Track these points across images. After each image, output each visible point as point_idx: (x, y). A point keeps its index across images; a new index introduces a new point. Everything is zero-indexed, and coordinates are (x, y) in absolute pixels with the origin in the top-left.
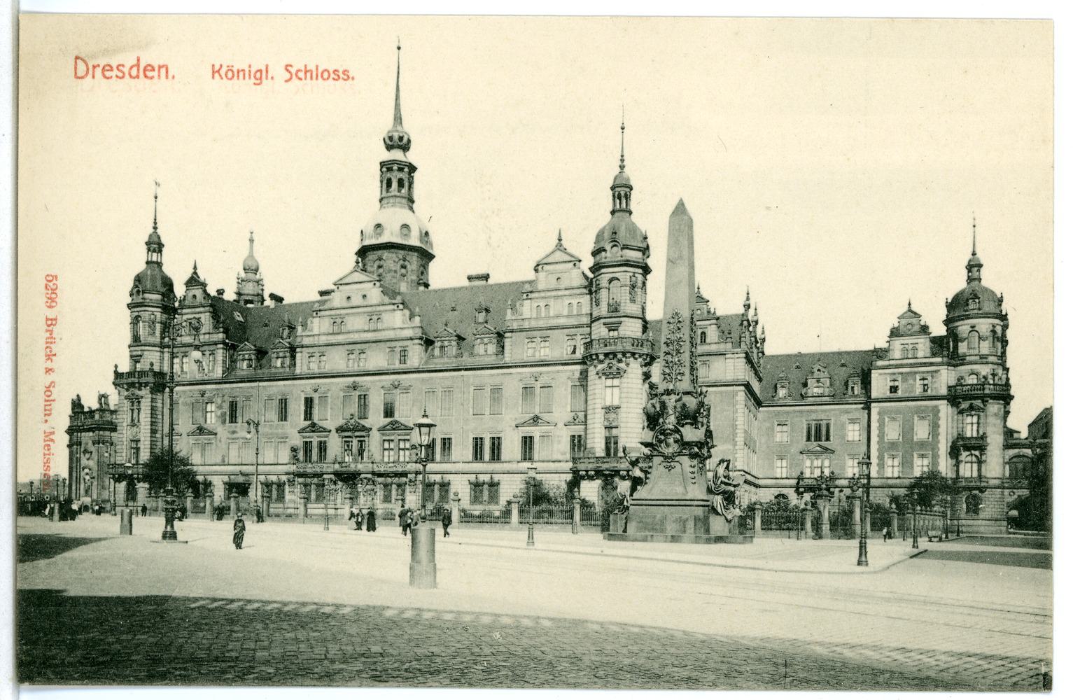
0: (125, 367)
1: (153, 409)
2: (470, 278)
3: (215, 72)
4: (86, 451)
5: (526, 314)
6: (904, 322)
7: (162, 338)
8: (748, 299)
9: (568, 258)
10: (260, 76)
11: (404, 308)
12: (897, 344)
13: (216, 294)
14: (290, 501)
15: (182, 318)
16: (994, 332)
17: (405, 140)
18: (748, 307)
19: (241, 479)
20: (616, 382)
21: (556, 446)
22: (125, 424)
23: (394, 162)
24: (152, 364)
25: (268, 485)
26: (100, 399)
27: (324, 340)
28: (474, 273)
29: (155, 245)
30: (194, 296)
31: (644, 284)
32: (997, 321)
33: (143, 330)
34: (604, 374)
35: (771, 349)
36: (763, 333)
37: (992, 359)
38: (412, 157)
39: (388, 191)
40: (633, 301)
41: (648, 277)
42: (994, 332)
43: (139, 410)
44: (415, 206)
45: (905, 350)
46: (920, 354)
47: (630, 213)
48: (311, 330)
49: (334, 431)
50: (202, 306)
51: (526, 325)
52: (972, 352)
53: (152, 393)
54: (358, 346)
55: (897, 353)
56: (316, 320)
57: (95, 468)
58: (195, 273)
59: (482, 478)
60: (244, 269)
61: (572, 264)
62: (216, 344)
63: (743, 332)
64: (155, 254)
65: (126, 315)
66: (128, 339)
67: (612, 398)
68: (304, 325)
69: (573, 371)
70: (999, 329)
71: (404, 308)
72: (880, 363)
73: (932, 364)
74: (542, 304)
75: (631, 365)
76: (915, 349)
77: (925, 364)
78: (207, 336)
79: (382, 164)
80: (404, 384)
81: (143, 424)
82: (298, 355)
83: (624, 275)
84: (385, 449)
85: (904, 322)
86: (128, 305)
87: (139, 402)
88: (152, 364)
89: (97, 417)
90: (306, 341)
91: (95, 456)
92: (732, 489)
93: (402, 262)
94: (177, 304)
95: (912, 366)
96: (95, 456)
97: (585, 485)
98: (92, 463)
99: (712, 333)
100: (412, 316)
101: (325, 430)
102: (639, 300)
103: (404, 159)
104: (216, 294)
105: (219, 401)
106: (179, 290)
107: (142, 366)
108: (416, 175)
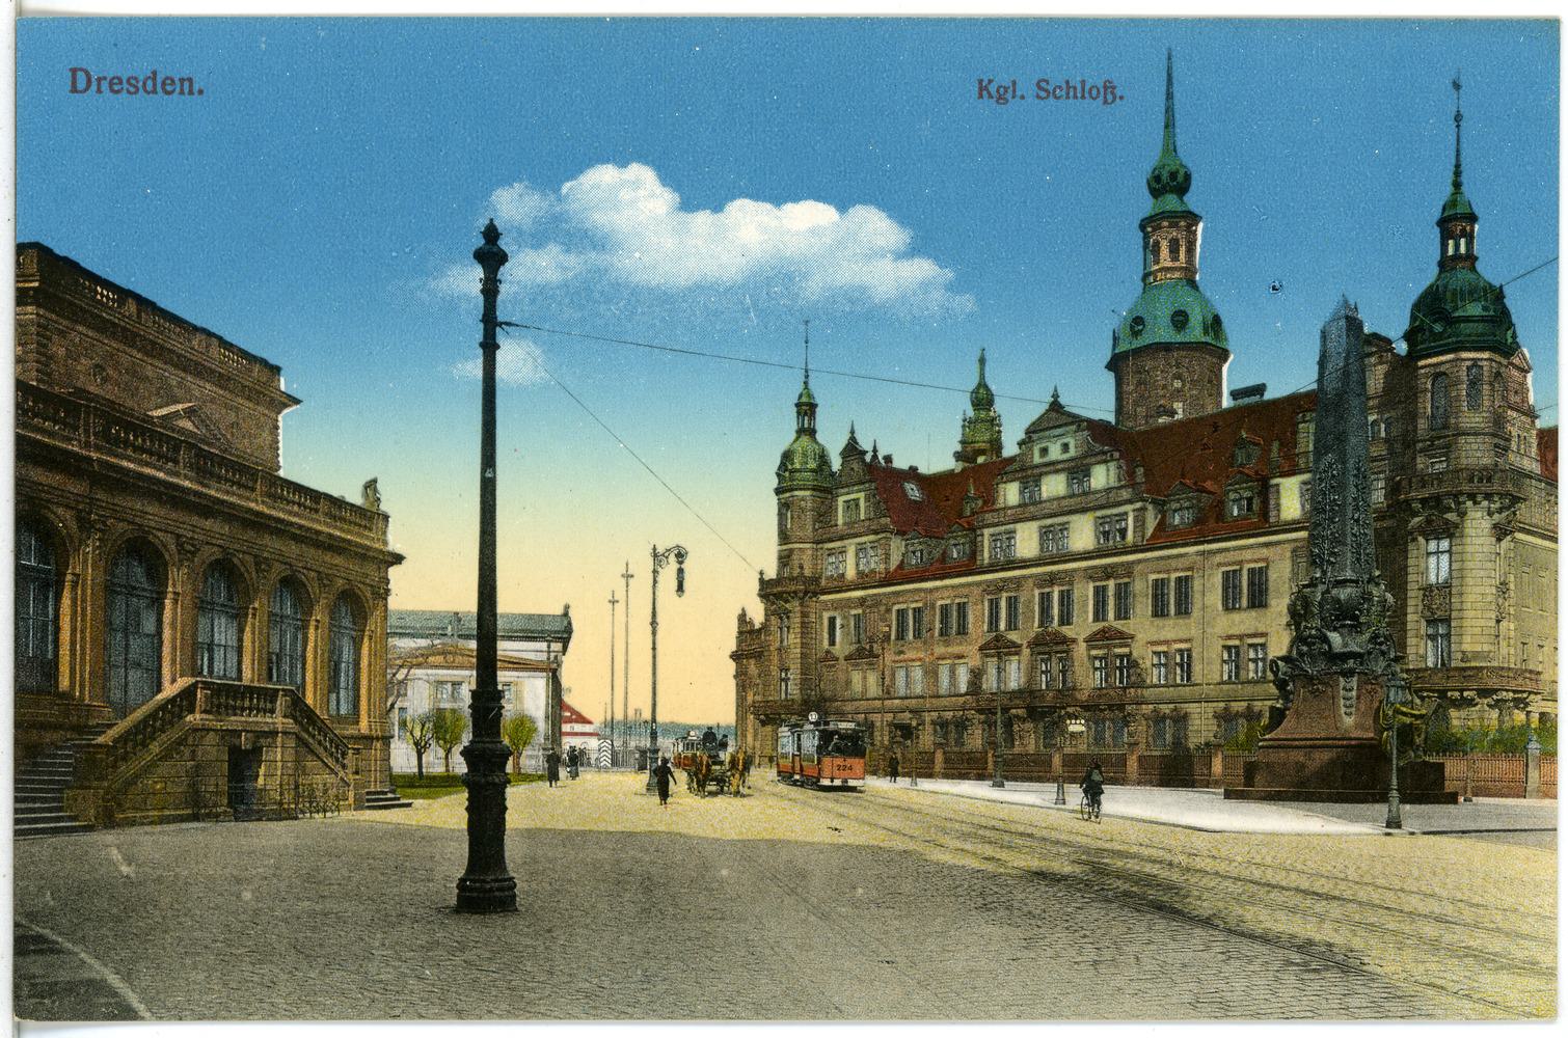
0: (771, 573)
3: (983, 89)
10: (1044, 89)
17: (1180, 178)
20: (1445, 544)
25: (943, 724)
40: (1471, 407)
59: (1166, 709)
67: (1437, 569)
71: (1121, 457)
75: (1471, 514)
84: (1096, 669)
87: (788, 618)
93: (1174, 370)
102: (1486, 403)
106: (836, 464)
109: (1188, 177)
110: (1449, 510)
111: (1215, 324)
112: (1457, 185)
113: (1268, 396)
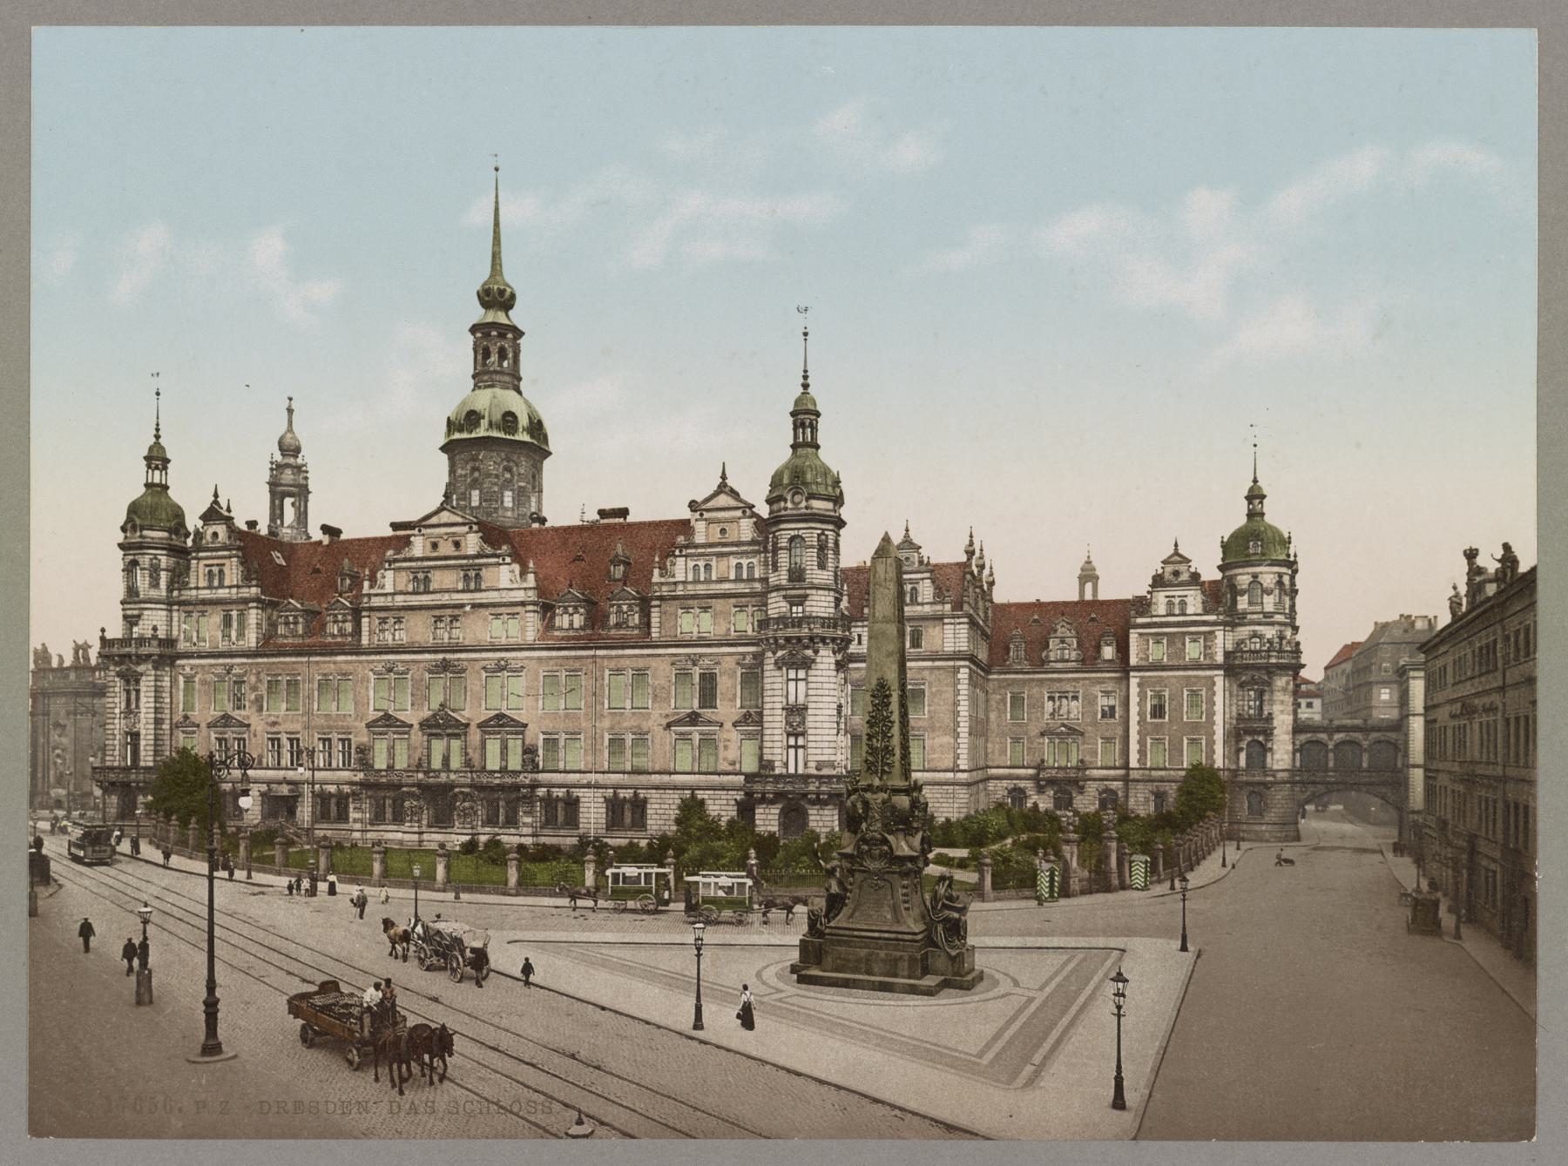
0: (116, 631)
1: (158, 691)
2: (602, 513)
4: (57, 725)
5: (680, 577)
6: (1169, 569)
7: (170, 590)
8: (971, 544)
9: (733, 503)
11: (514, 561)
12: (1161, 598)
13: (244, 528)
14: (355, 821)
15: (198, 572)
16: (1280, 583)
18: (970, 553)
19: (285, 790)
20: (801, 674)
21: (722, 753)
22: (117, 711)
23: (494, 325)
24: (155, 629)
25: (322, 799)
26: (76, 652)
27: (400, 600)
28: (608, 506)
29: (157, 459)
30: (215, 535)
31: (837, 543)
32: (1284, 570)
33: (142, 581)
34: (785, 664)
35: (1000, 596)
36: (991, 574)
37: (1279, 618)
38: (517, 317)
39: (484, 364)
40: (822, 566)
41: (842, 532)
42: (1280, 583)
43: (138, 691)
44: (523, 385)
45: (1170, 604)
46: (1190, 610)
47: (817, 447)
48: (383, 587)
49: (416, 727)
50: (224, 548)
51: (680, 591)
52: (1252, 609)
53: (156, 668)
54: (449, 612)
55: (1160, 608)
56: (389, 574)
57: (71, 748)
58: (216, 502)
60: (281, 449)
61: (739, 513)
62: (245, 601)
63: (965, 584)
64: (157, 473)
65: (117, 559)
66: (120, 593)
68: (373, 580)
69: (744, 655)
70: (1286, 580)
72: (1140, 620)
73: (1204, 623)
74: (701, 564)
76: (1183, 604)
77: (1194, 623)
78: (234, 590)
79: (474, 329)
80: (513, 665)
81: (143, 710)
82: (365, 621)
83: (811, 534)
85: (1169, 569)
86: (121, 546)
87: (137, 682)
88: (155, 629)
89: (72, 676)
90: (377, 602)
91: (70, 729)
92: (956, 915)
94: (189, 542)
95: (1178, 624)
96: (70, 729)
97: (760, 811)
98: (64, 740)
99: (926, 590)
100: (523, 573)
101: (404, 724)
103: (506, 322)
104: (244, 528)
105: (253, 679)
106: (193, 522)
107: (142, 629)
108: (522, 341)
109: (513, 296)
110: (807, 647)
111: (536, 427)
112: (806, 386)
113: (630, 519)
